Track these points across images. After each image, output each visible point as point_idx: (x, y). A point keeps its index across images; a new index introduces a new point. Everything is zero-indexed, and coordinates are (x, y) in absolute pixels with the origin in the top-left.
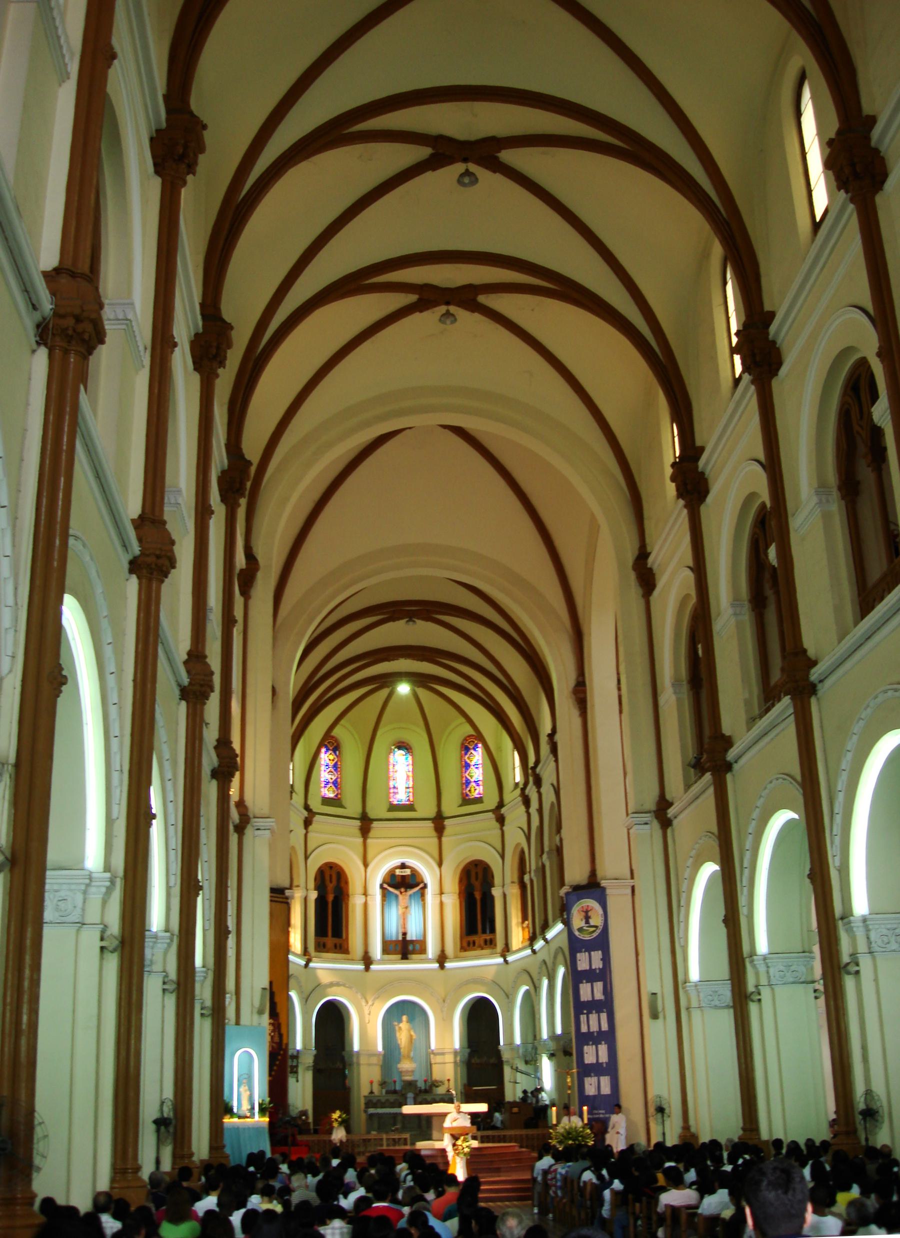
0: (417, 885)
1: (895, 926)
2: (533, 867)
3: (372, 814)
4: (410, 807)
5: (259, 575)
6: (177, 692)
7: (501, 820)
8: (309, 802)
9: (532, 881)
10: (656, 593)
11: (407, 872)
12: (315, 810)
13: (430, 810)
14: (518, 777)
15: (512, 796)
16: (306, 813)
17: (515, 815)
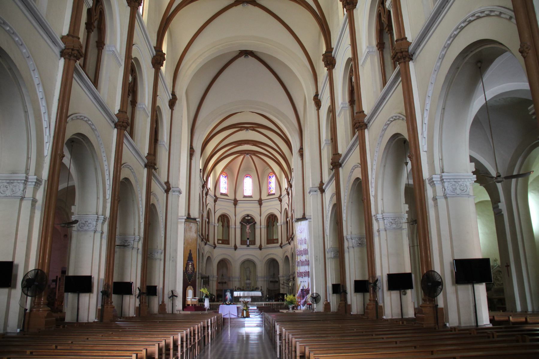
0: (252, 222)
1: (395, 218)
2: (290, 216)
3: (238, 198)
4: (251, 197)
5: (177, 102)
6: (113, 125)
7: (281, 201)
8: (216, 194)
9: (289, 220)
10: (321, 108)
11: (250, 218)
12: (218, 197)
13: (258, 198)
14: (286, 187)
15: (284, 193)
16: (215, 198)
17: (285, 199)
